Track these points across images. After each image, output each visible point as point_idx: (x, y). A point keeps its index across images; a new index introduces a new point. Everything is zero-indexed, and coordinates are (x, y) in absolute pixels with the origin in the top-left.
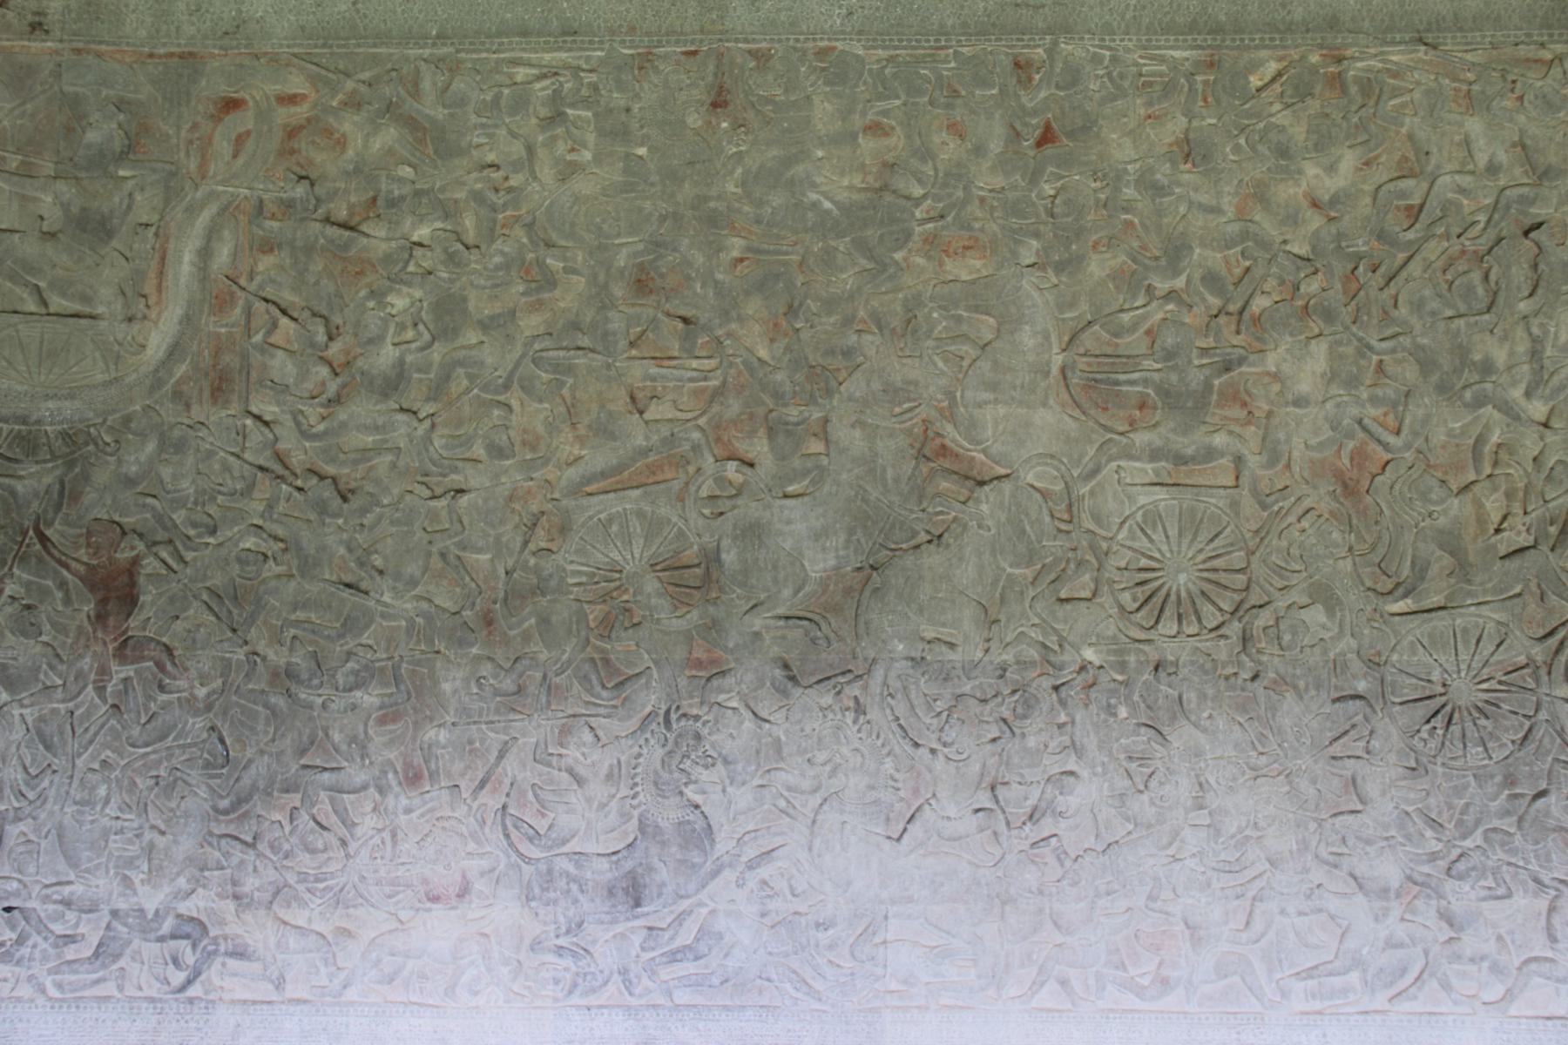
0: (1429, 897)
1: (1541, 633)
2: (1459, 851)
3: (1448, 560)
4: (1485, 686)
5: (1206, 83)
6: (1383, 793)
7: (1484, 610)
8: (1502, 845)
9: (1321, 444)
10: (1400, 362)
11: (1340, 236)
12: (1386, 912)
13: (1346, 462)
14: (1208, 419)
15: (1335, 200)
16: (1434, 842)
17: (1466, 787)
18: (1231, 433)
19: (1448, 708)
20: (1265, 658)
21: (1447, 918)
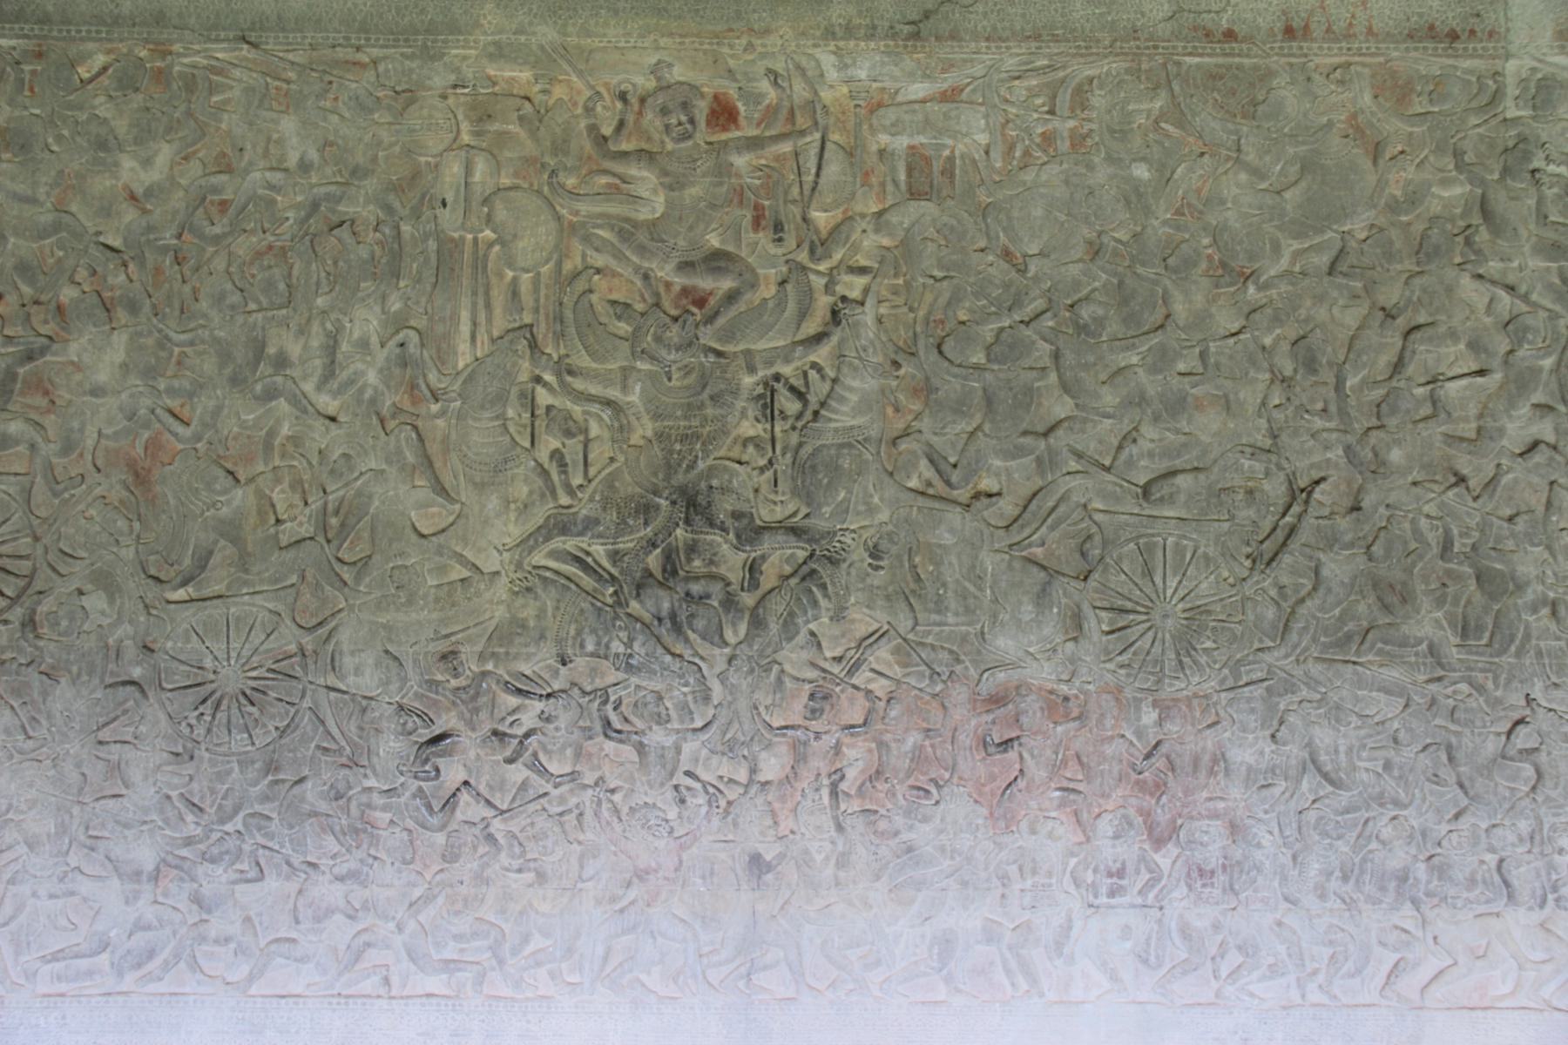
0: (182, 879)
1: (314, 621)
2: (219, 835)
3: (230, 550)
4: (254, 674)
5: (34, 72)
6: (146, 778)
7: (258, 599)
8: (259, 829)
9: (115, 433)
10: (200, 354)
11: (150, 229)
12: (136, 895)
13: (140, 450)
14: (9, 407)
15: (149, 192)
16: (193, 826)
17: (229, 772)
18: (28, 420)
19: (218, 695)
20: (41, 643)
21: (197, 899)
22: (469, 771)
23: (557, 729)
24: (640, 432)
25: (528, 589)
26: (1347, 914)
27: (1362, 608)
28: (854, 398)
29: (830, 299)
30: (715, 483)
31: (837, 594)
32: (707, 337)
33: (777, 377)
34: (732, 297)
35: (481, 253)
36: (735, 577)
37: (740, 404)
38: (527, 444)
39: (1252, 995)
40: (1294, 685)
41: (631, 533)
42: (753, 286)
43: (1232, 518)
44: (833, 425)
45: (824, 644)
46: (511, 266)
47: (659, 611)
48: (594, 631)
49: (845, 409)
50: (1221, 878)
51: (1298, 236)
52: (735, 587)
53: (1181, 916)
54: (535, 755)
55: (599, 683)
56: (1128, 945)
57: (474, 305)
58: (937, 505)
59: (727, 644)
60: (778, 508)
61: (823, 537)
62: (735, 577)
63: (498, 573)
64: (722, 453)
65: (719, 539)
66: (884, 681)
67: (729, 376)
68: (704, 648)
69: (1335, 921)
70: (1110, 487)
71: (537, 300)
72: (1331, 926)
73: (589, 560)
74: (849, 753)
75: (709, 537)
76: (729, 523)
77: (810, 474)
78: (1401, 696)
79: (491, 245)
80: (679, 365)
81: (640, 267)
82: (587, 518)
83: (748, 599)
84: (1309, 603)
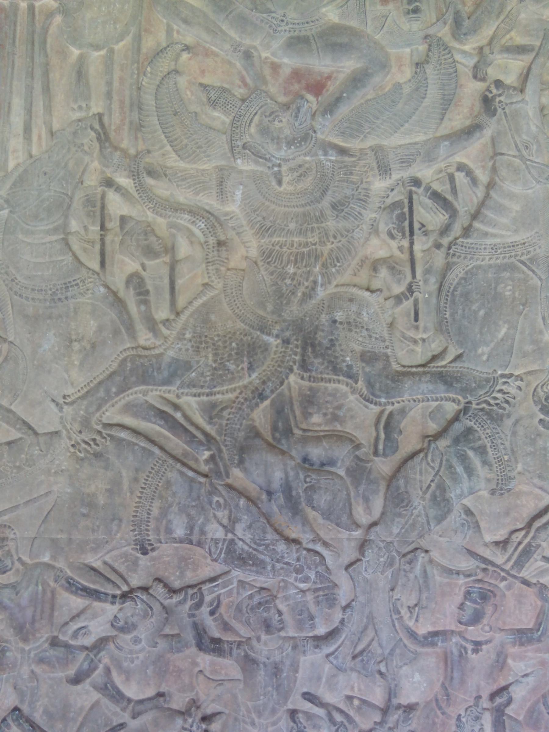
22: (21, 695)
23: (136, 640)
24: (242, 251)
25: (97, 455)
28: (516, 207)
29: (480, 86)
30: (339, 316)
31: (500, 460)
32: (326, 130)
33: (417, 182)
34: (358, 80)
35: (38, 27)
36: (365, 437)
37: (369, 215)
38: (95, 265)
41: (233, 380)
42: (384, 66)
44: (490, 241)
45: (482, 524)
46: (75, 40)
47: (269, 482)
48: (183, 510)
49: (504, 220)
52: (366, 450)
54: (108, 671)
55: (190, 577)
57: (30, 90)
59: (358, 526)
60: (419, 349)
61: (480, 387)
62: (365, 437)
63: (57, 433)
64: (346, 278)
65: (343, 388)
67: (355, 178)
68: (327, 530)
71: (109, 84)
73: (178, 415)
74: (516, 666)
75: (331, 386)
76: (358, 367)
77: (459, 304)
79: (50, 15)
80: (292, 164)
81: (240, 44)
82: (175, 361)
83: (383, 466)
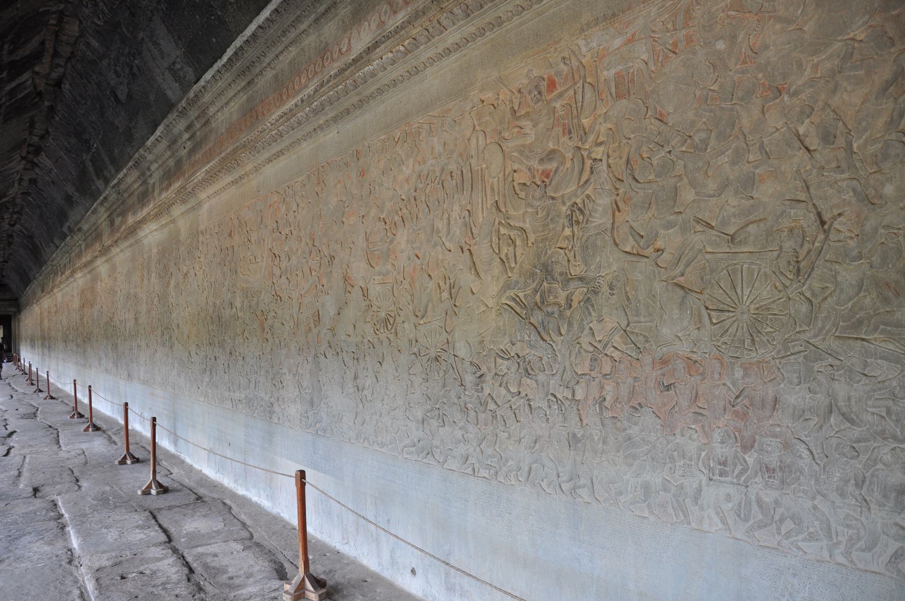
26: (859, 510)
27: (868, 301)
28: (601, 209)
30: (553, 260)
39: (799, 548)
40: (820, 355)
43: (781, 247)
50: (779, 474)
51: (816, 52)
53: (757, 493)
56: (730, 505)
58: (635, 259)
66: (618, 352)
69: (852, 513)
70: (714, 238)
72: (848, 515)
74: (607, 388)
78: (897, 362)
84: (829, 300)
